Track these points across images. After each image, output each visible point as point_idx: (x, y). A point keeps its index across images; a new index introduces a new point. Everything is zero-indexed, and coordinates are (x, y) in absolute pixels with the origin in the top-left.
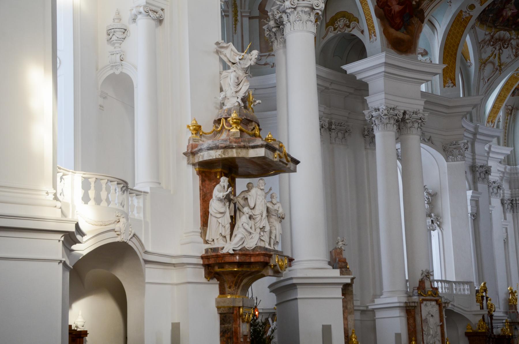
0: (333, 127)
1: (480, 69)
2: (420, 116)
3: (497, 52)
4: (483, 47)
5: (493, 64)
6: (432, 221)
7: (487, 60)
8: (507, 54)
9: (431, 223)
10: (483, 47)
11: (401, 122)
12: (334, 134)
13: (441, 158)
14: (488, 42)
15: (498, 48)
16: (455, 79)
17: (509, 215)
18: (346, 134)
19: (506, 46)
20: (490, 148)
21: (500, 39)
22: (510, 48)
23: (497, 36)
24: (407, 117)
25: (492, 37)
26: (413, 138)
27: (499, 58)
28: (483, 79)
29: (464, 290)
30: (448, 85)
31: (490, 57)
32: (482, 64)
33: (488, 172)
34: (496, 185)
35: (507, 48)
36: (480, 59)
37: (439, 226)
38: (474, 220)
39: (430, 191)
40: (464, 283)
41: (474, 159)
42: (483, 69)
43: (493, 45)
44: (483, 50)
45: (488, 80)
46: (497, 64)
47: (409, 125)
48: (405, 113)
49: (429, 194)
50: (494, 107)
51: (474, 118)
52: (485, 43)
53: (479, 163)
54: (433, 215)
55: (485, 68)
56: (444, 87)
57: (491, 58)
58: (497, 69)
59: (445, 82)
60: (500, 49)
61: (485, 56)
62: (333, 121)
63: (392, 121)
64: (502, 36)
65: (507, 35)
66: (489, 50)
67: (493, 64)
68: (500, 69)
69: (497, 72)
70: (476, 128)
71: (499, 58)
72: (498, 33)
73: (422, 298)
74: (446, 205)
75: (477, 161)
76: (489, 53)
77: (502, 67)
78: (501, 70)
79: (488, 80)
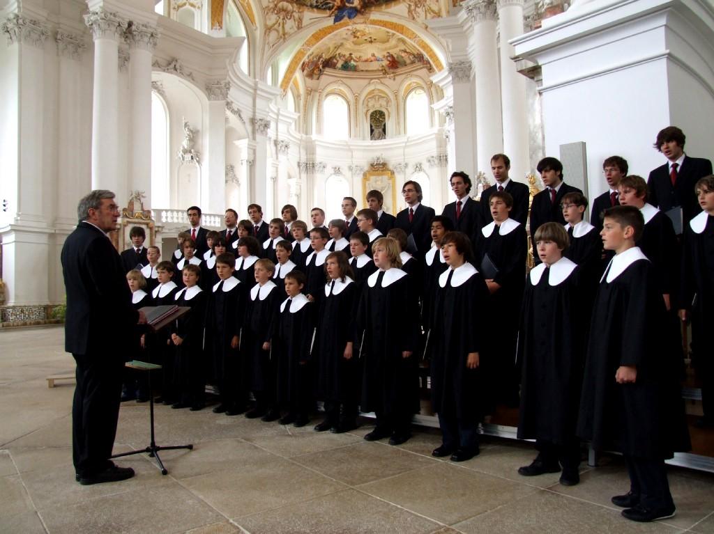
0: (59, 37)
1: (265, 34)
2: (150, 30)
3: (281, 21)
4: (267, 13)
5: (278, 31)
6: (192, 157)
7: (271, 27)
8: (290, 25)
9: (190, 159)
10: (267, 13)
11: (128, 32)
12: (61, 45)
13: (203, 96)
14: (272, 10)
15: (281, 17)
16: (222, 22)
17: (304, 175)
18: (80, 50)
19: (289, 17)
20: (279, 110)
21: (283, 10)
22: (292, 19)
23: (280, 5)
24: (134, 28)
25: (276, 6)
26: (143, 55)
27: (283, 27)
28: (268, 43)
29: (215, 222)
30: (215, 27)
31: (274, 25)
32: (268, 29)
33: (266, 126)
34: (284, 144)
35: (290, 19)
36: (266, 25)
37: (198, 162)
38: (250, 166)
39: (191, 128)
40: (214, 215)
41: (254, 112)
42: (268, 35)
43: (276, 14)
44: (267, 17)
45: (273, 45)
46: (281, 33)
47: (137, 38)
48: (130, 24)
49: (191, 131)
50: (285, 77)
51: (258, 76)
52: (269, 10)
53: (258, 116)
54: (192, 150)
55: (271, 34)
56: (212, 29)
57: (276, 26)
58: (281, 37)
59: (212, 24)
60: (284, 19)
61: (270, 23)
62: (60, 30)
63: (113, 29)
64: (285, 8)
65: (290, 7)
66: (272, 19)
67: (278, 31)
68: (284, 36)
69: (282, 40)
70: (256, 84)
71: (283, 27)
72: (281, 3)
73: (126, 219)
74: (206, 143)
75: (257, 114)
76: (274, 21)
77: (286, 36)
78: (284, 39)
79: (273, 45)
